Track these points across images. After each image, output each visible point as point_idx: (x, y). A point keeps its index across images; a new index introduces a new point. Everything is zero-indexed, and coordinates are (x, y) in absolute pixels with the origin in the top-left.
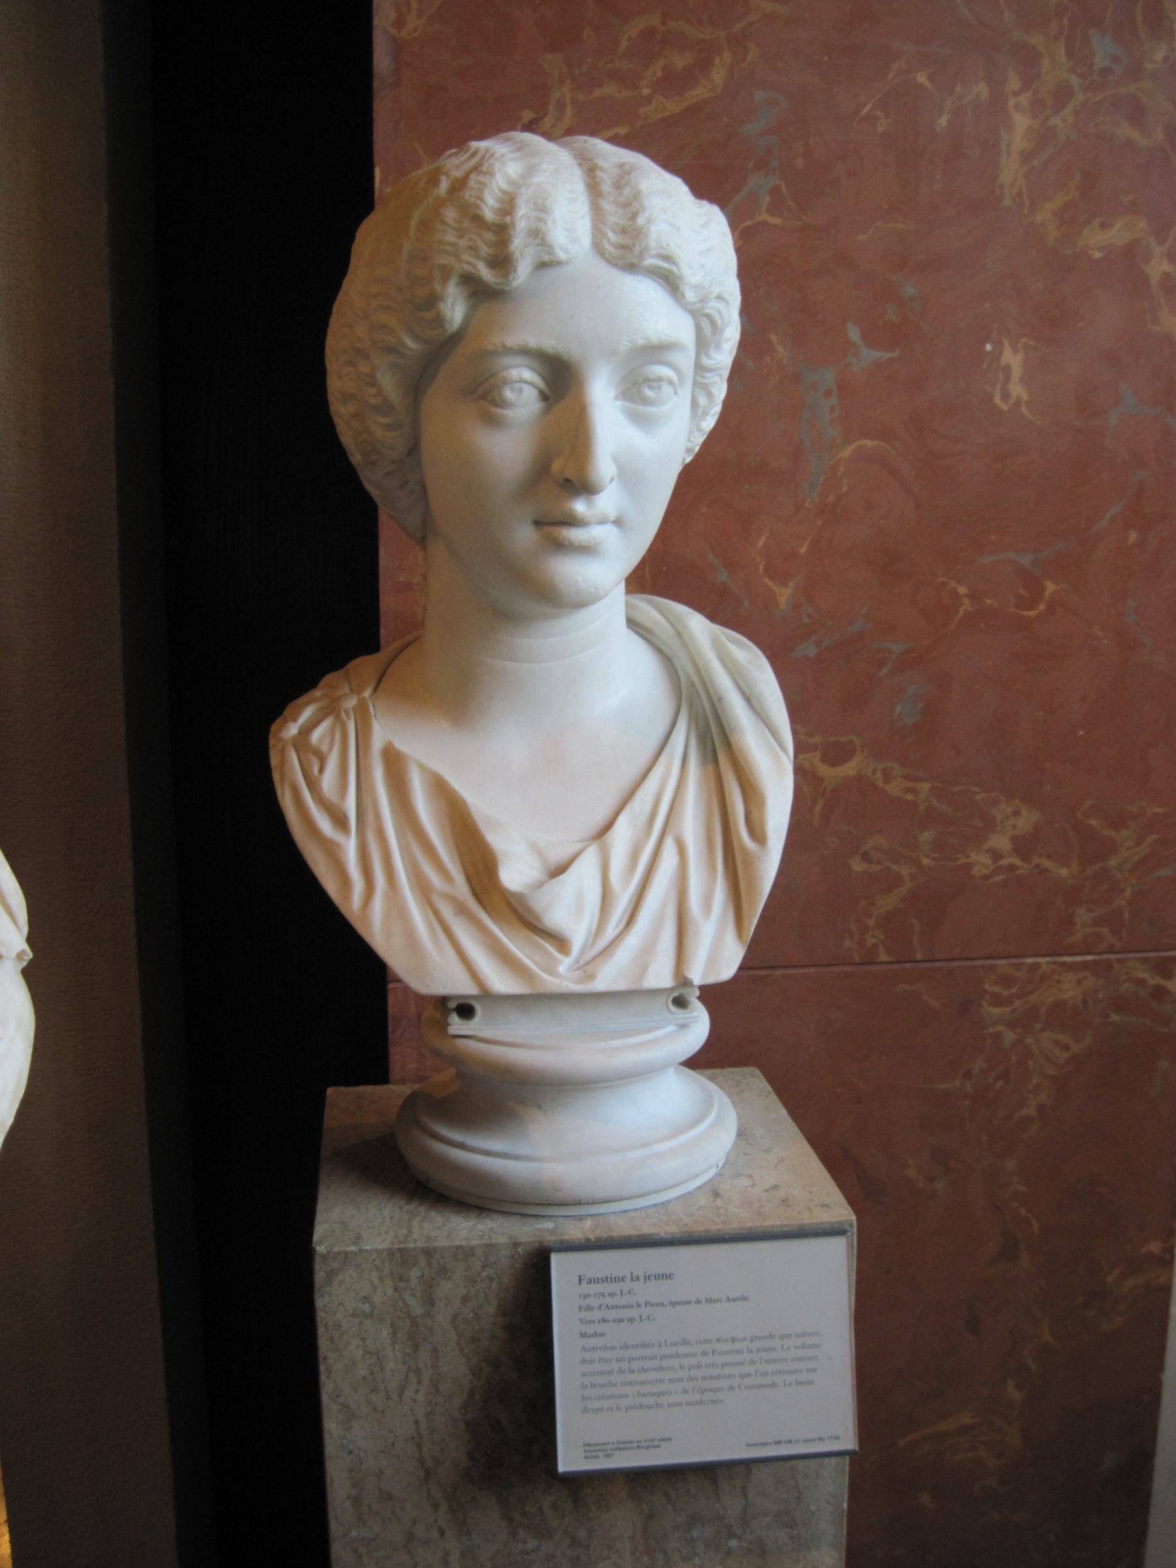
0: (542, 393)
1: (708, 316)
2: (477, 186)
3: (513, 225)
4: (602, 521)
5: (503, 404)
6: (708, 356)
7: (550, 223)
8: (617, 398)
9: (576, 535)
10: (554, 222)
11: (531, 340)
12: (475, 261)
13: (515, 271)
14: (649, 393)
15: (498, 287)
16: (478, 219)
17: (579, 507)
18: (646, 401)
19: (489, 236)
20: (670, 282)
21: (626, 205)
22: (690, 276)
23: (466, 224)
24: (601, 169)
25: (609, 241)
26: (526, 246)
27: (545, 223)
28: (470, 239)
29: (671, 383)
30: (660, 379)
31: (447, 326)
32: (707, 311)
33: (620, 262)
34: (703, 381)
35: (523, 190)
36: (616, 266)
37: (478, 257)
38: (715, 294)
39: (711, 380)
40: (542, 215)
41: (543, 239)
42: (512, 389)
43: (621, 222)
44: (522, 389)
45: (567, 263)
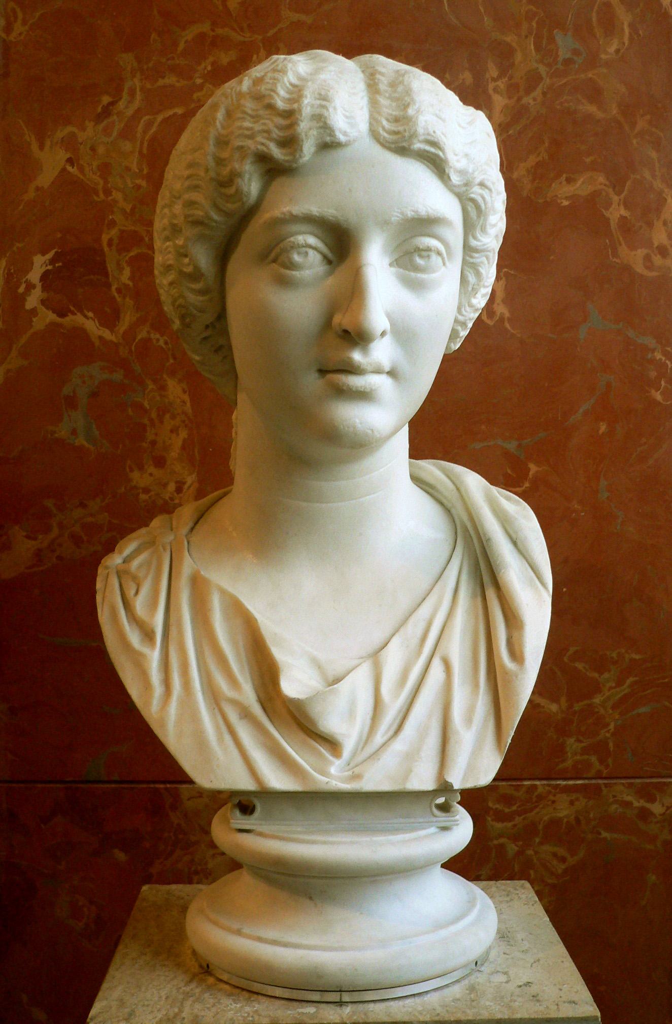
0: (325, 257)
1: (473, 200)
2: (271, 81)
3: (300, 110)
4: (378, 371)
5: (292, 266)
6: (475, 238)
7: (331, 110)
8: (391, 265)
9: (355, 381)
10: (335, 109)
11: (315, 209)
13: (301, 150)
14: (420, 261)
15: (287, 164)
16: (271, 107)
17: (357, 356)
18: (417, 269)
19: (281, 121)
20: (436, 163)
21: (397, 99)
22: (455, 160)
23: (261, 112)
24: (380, 73)
25: (384, 128)
26: (310, 129)
27: (328, 110)
28: (264, 124)
29: (439, 253)
30: (428, 249)
31: (245, 199)
32: (472, 196)
33: (393, 146)
34: (472, 260)
35: (310, 83)
36: (390, 149)
37: (271, 139)
38: (478, 181)
39: (478, 260)
40: (324, 103)
41: (325, 123)
42: (299, 253)
43: (394, 113)
44: (309, 253)
45: (346, 145)
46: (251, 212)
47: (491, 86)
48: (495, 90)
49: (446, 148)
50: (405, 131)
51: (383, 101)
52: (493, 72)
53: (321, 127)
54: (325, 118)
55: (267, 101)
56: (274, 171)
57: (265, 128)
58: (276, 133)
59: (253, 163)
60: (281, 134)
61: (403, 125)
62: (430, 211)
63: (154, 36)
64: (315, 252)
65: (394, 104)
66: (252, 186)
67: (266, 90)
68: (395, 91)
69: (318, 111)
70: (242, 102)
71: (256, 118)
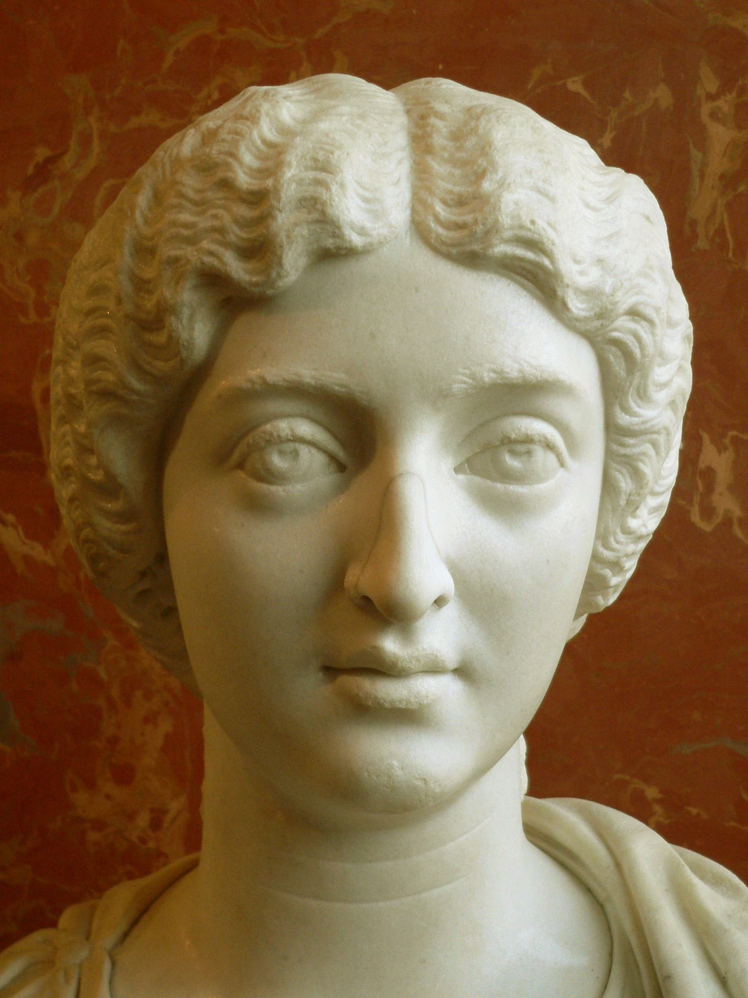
0: (332, 457)
1: (617, 343)
3: (277, 191)
4: (434, 669)
5: (269, 476)
6: (626, 410)
7: (334, 188)
8: (458, 470)
9: (390, 691)
10: (342, 186)
11: (306, 372)
12: (220, 250)
13: (280, 264)
14: (512, 462)
15: (256, 290)
16: (226, 184)
17: (390, 645)
18: (507, 476)
19: (243, 211)
20: (539, 280)
21: (463, 164)
22: (576, 272)
23: (210, 195)
25: (437, 219)
26: (296, 225)
27: (328, 189)
28: (215, 217)
29: (549, 446)
30: (528, 440)
31: (184, 354)
32: (616, 334)
34: (623, 451)
35: (298, 140)
36: (448, 257)
37: (226, 245)
38: (624, 307)
39: (636, 450)
40: (322, 176)
41: (323, 213)
42: (281, 453)
43: (457, 189)
44: (301, 451)
47: (706, 109)
48: (713, 115)
49: (555, 251)
50: (476, 222)
51: (438, 167)
52: (709, 82)
53: (317, 221)
54: (324, 204)
55: (220, 174)
56: (235, 303)
57: (216, 223)
58: (236, 234)
59: (195, 287)
60: (244, 235)
61: (474, 211)
62: (527, 369)
63: (122, 44)
64: (314, 451)
65: (458, 172)
66: (196, 330)
67: (220, 152)
68: (460, 148)
69: (310, 191)
70: (181, 177)
71: (202, 206)
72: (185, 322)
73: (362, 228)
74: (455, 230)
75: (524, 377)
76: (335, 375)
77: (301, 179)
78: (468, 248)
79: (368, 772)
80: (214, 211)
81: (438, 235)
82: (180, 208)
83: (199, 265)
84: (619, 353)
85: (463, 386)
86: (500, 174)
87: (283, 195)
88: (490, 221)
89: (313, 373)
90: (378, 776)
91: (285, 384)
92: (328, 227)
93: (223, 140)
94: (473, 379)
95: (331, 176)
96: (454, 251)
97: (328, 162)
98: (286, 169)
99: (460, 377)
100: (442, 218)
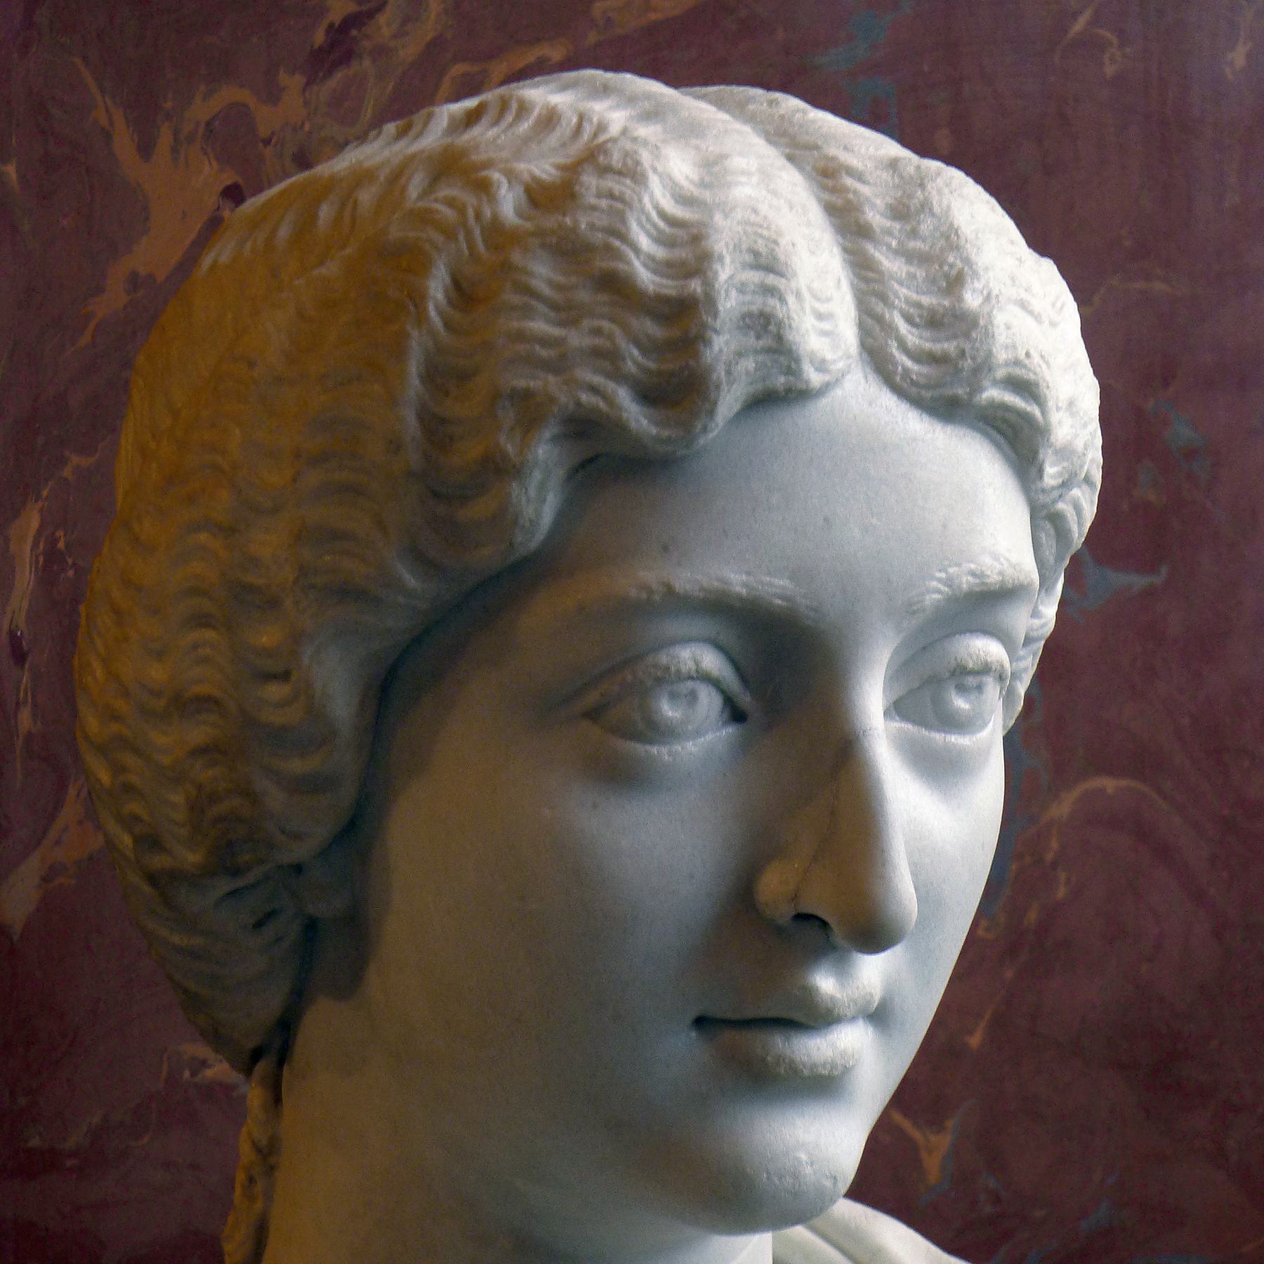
2: (604, 203)
5: (655, 731)
7: (791, 300)
10: (798, 295)
11: (736, 579)
12: (610, 386)
14: (961, 703)
16: (616, 286)
19: (650, 328)
24: (850, 171)
26: (740, 354)
27: (782, 300)
28: (597, 332)
31: (519, 538)
33: (927, 394)
36: (917, 402)
37: (618, 376)
40: (771, 279)
41: (779, 338)
42: (673, 697)
43: (926, 300)
46: (526, 574)
50: (962, 353)
51: (891, 265)
53: (768, 351)
54: (780, 324)
55: (601, 264)
56: (611, 466)
57: (598, 341)
58: (634, 360)
59: (555, 439)
60: (652, 365)
61: (955, 337)
62: (1009, 571)
64: (714, 692)
65: (921, 274)
66: (539, 498)
67: (592, 226)
68: (914, 233)
69: (757, 304)
70: (516, 257)
71: (568, 313)
72: (532, 492)
73: (823, 361)
74: (929, 364)
75: (1002, 581)
76: (777, 581)
77: (743, 284)
78: (949, 392)
79: (768, 1173)
80: (596, 323)
81: (906, 371)
82: (527, 312)
83: (571, 406)
84: (1052, 532)
85: (936, 596)
86: (983, 281)
87: (721, 308)
88: (982, 354)
89: (744, 577)
90: (780, 1179)
91: (702, 595)
92: (782, 358)
93: (594, 208)
94: (950, 586)
95: (783, 280)
96: (927, 394)
97: (775, 258)
98: (717, 266)
99: (934, 584)
100: (910, 344)
